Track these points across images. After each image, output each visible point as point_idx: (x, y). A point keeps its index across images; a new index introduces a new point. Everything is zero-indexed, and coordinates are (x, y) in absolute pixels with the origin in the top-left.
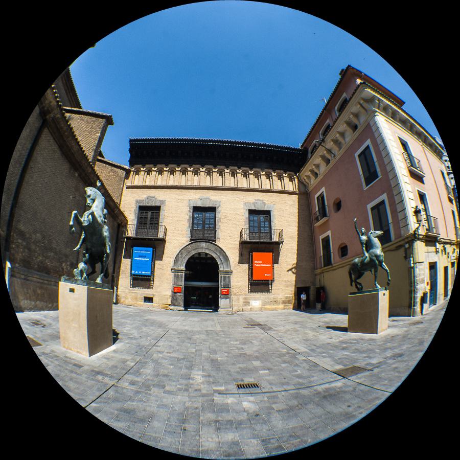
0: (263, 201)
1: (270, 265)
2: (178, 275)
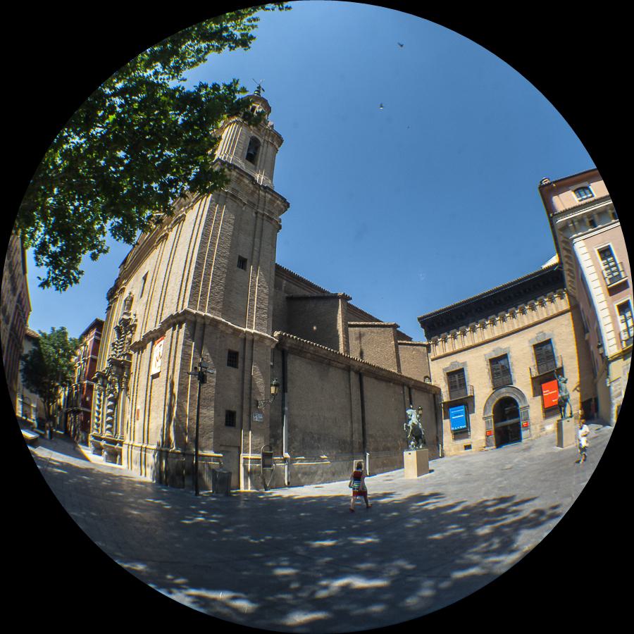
0: (542, 332)
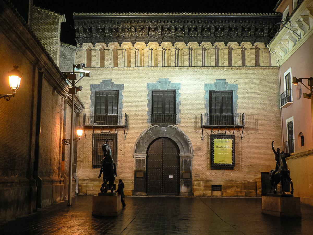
0: (225, 80)
2: (140, 160)
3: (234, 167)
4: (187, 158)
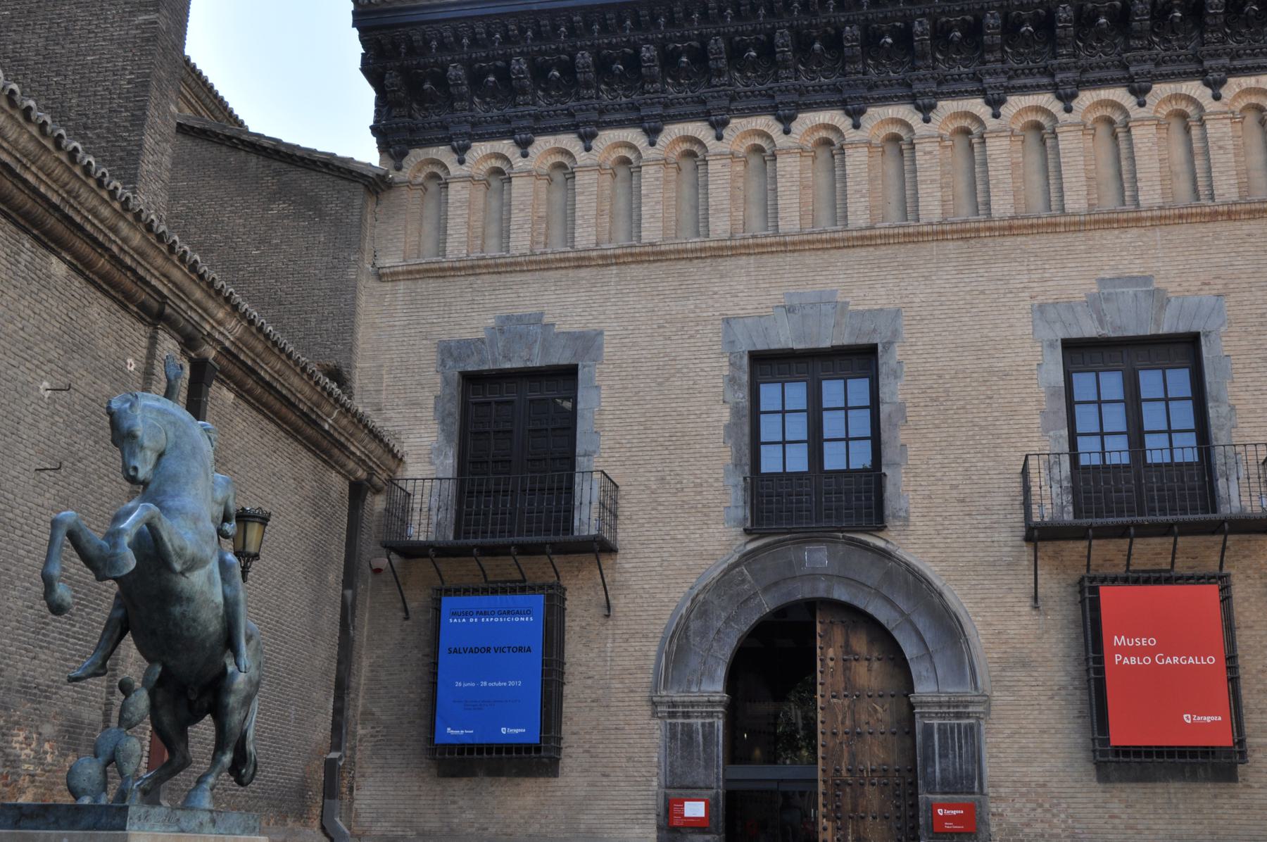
0: (1147, 280)
1: (1211, 660)
2: (689, 731)
3: (1240, 768)
4: (958, 715)
